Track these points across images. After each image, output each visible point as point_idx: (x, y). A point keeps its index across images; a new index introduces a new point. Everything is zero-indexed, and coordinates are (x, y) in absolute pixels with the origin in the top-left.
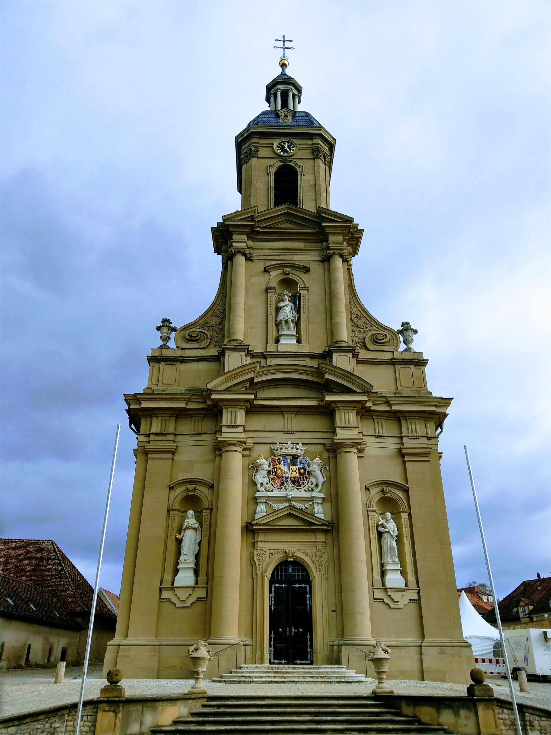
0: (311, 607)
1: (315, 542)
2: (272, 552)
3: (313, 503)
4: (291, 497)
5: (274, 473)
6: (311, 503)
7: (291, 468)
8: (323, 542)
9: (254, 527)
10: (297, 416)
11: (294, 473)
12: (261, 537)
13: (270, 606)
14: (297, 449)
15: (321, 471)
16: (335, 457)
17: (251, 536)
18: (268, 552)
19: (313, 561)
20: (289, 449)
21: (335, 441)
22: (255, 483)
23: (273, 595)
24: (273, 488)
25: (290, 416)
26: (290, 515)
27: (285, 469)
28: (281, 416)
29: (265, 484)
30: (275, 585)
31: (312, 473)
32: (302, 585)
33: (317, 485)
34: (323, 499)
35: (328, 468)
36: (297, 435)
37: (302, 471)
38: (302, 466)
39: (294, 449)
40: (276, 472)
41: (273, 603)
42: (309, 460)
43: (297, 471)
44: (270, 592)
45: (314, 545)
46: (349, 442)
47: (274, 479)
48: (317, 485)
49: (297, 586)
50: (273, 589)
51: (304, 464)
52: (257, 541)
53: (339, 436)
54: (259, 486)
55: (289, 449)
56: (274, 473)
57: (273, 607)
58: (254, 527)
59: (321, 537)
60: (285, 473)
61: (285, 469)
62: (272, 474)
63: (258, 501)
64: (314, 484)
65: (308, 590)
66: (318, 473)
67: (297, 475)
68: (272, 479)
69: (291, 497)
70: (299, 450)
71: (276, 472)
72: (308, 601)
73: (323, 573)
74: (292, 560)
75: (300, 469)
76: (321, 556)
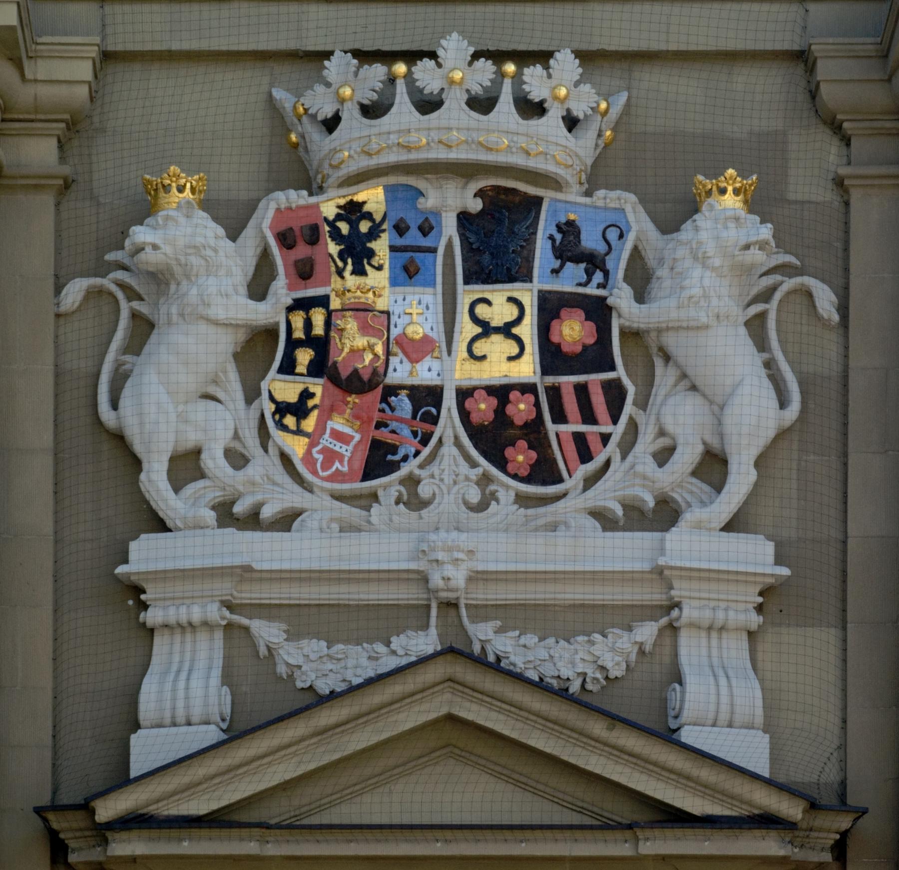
4: (459, 577)
5: (304, 357)
11: (497, 348)
15: (756, 327)
27: (416, 311)
33: (713, 466)
38: (571, 280)
40: (310, 341)
42: (640, 224)
43: (527, 330)
47: (300, 409)
48: (713, 466)
64: (687, 456)
67: (527, 369)
68: (282, 409)
71: (321, 346)
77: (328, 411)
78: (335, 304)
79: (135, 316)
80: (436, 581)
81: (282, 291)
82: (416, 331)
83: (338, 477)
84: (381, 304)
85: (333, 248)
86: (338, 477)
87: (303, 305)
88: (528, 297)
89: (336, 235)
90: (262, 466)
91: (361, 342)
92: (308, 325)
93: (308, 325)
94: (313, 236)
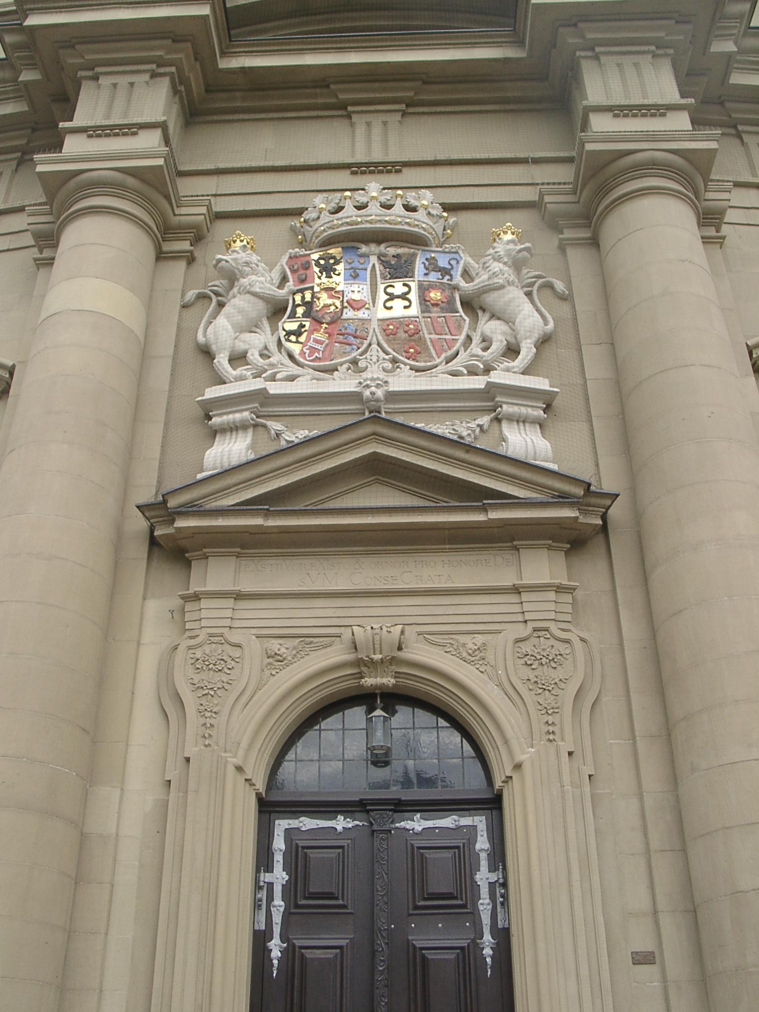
0: (503, 937)
1: (516, 590)
2: (274, 645)
3: (498, 420)
4: (380, 393)
5: (300, 311)
6: (485, 420)
7: (381, 287)
8: (559, 589)
9: (181, 523)
10: (410, 121)
11: (398, 304)
12: (217, 574)
13: (260, 939)
14: (409, 208)
15: (529, 294)
16: (594, 242)
17: (167, 576)
18: (254, 648)
19: (513, 694)
20: (374, 209)
21: (589, 147)
22: (207, 353)
23: (279, 876)
24: (294, 369)
25: (377, 121)
26: (377, 469)
27: (358, 291)
28: (346, 122)
29: (254, 356)
30: (294, 823)
31: (490, 299)
32: (448, 821)
33: (512, 351)
34: (548, 402)
35: (560, 286)
36: (410, 176)
37: (435, 295)
38: (434, 277)
39: (398, 209)
40: (305, 303)
41: (277, 919)
42: (466, 259)
43: (413, 296)
44: (264, 860)
45: (506, 605)
46: (649, 151)
47: (298, 333)
48: (512, 351)
49: (417, 824)
50: (279, 843)
51: (445, 272)
52: (196, 597)
53: (600, 124)
54: (222, 361)
55: (374, 209)
56: (300, 311)
57: (276, 948)
58: (181, 523)
59: (541, 567)
60: (356, 305)
61: (358, 291)
62: (293, 315)
63: (216, 420)
64: (497, 346)
65: (482, 843)
66: (514, 298)
67: (414, 310)
68: (289, 333)
69: (380, 393)
70: (421, 215)
71: (309, 305)
72: (484, 905)
73: (566, 747)
74: (388, 681)
75: (423, 289)
76: (554, 661)
77: (311, 332)
78: (317, 289)
79: (218, 301)
80: (367, 393)
81: (291, 285)
82: (356, 297)
83: (317, 359)
84: (339, 288)
85: (317, 269)
86: (317, 359)
87: (302, 291)
88: (413, 285)
89: (318, 264)
90: (277, 357)
91: (330, 301)
92: (303, 298)
93: (303, 298)
94: (307, 266)
